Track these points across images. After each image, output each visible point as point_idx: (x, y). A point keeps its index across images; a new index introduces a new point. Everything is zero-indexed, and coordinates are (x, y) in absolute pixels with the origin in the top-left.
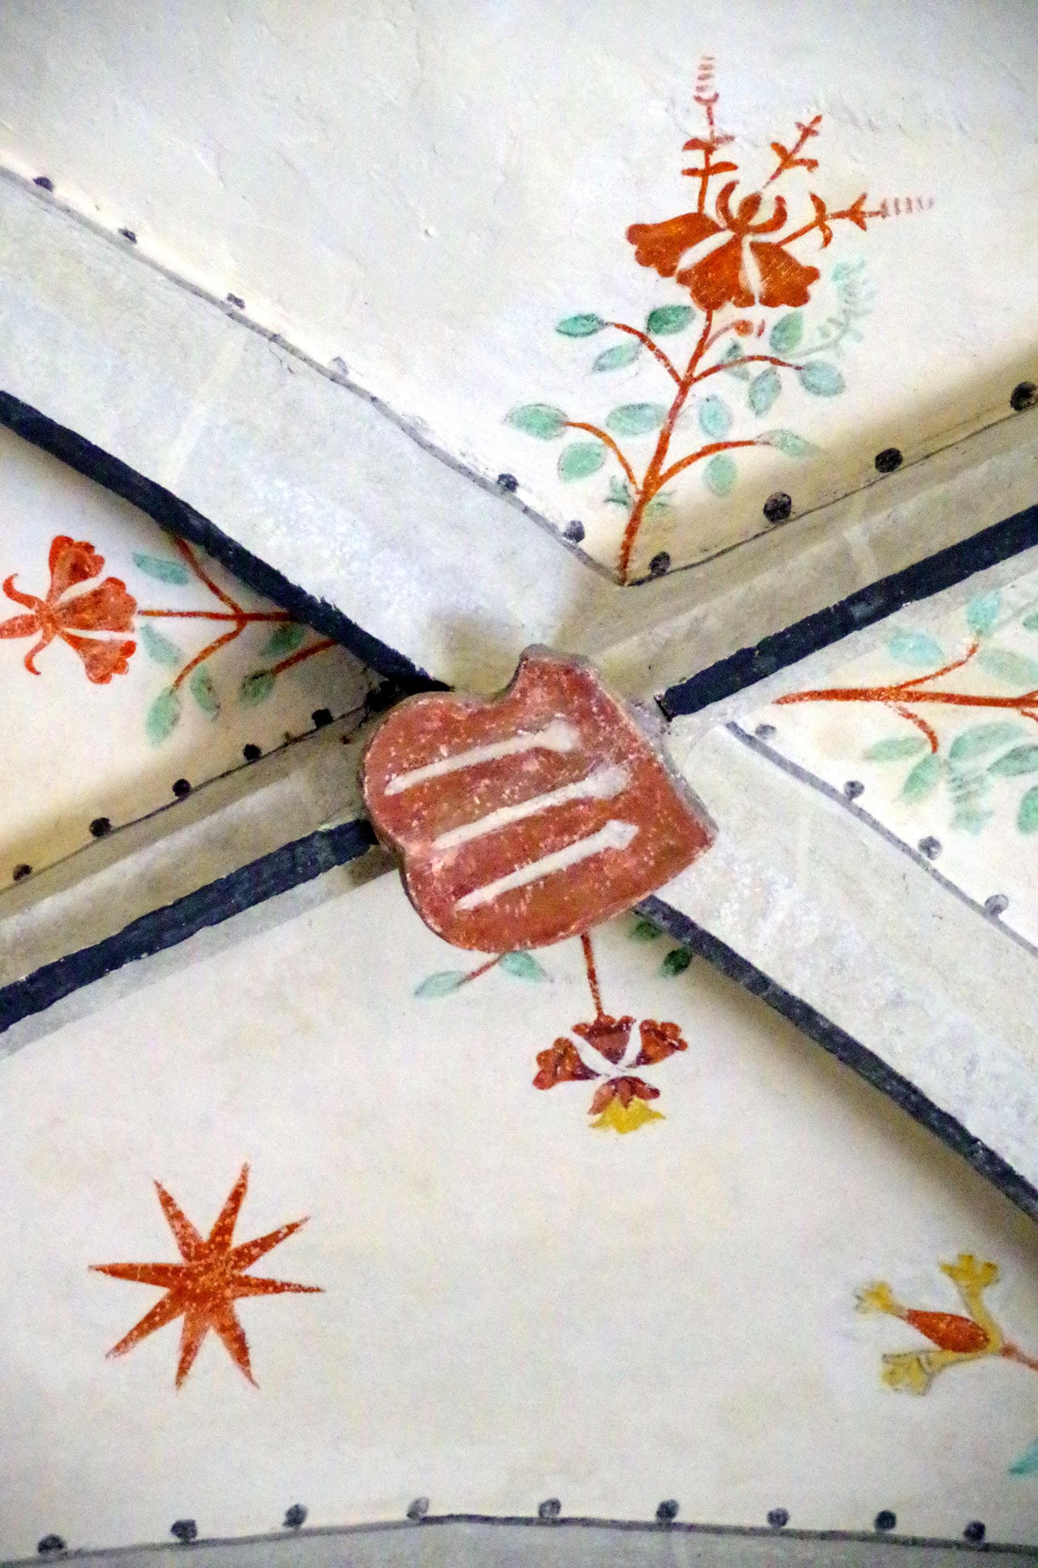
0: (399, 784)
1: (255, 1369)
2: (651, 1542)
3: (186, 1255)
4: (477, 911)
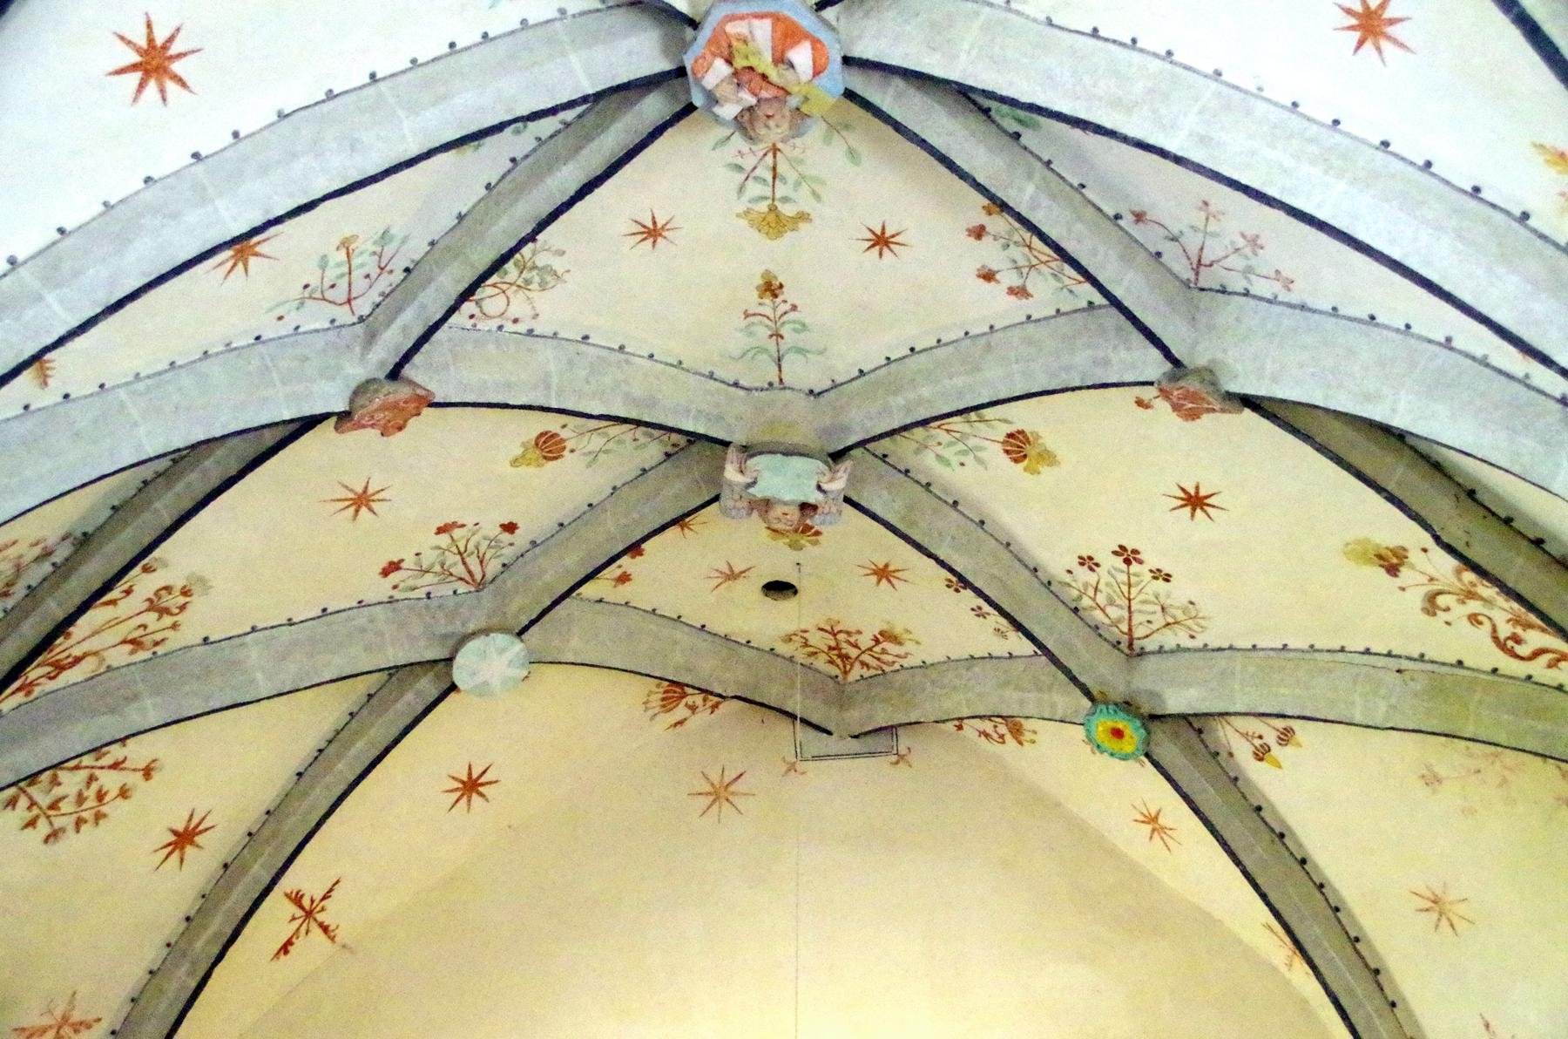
2: (372, 90)
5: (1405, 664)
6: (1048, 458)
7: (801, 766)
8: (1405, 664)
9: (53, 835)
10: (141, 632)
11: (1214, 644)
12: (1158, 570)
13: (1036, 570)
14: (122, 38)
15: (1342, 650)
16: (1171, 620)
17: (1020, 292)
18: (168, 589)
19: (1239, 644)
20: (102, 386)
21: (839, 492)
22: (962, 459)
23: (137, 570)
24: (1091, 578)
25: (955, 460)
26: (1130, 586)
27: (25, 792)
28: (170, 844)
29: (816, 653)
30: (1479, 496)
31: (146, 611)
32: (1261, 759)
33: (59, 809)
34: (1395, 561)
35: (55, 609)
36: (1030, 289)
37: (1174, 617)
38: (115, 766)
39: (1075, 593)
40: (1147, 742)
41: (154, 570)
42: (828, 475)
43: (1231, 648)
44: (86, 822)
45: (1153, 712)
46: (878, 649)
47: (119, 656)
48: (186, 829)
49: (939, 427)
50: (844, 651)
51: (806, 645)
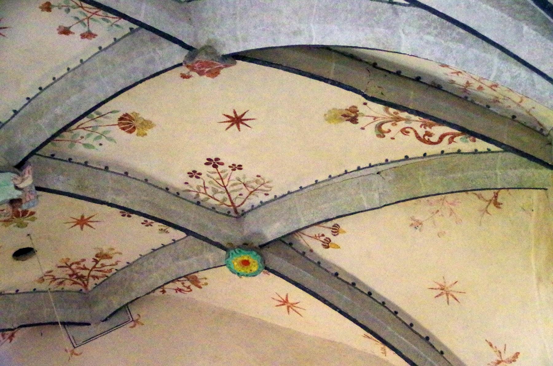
5: (380, 168)
6: (148, 124)
7: (77, 351)
8: (380, 168)
11: (279, 194)
12: (233, 165)
13: (167, 189)
15: (346, 172)
16: (252, 190)
17: (88, 35)
19: (292, 190)
21: (30, 186)
22: (101, 141)
24: (200, 182)
25: (96, 144)
26: (222, 179)
29: (63, 281)
30: (379, 65)
32: (328, 247)
34: (353, 115)
36: (93, 32)
37: (252, 187)
39: (194, 194)
40: (263, 261)
42: (19, 179)
43: (289, 193)
45: (261, 244)
46: (98, 265)
49: (78, 128)
50: (79, 274)
51: (54, 279)
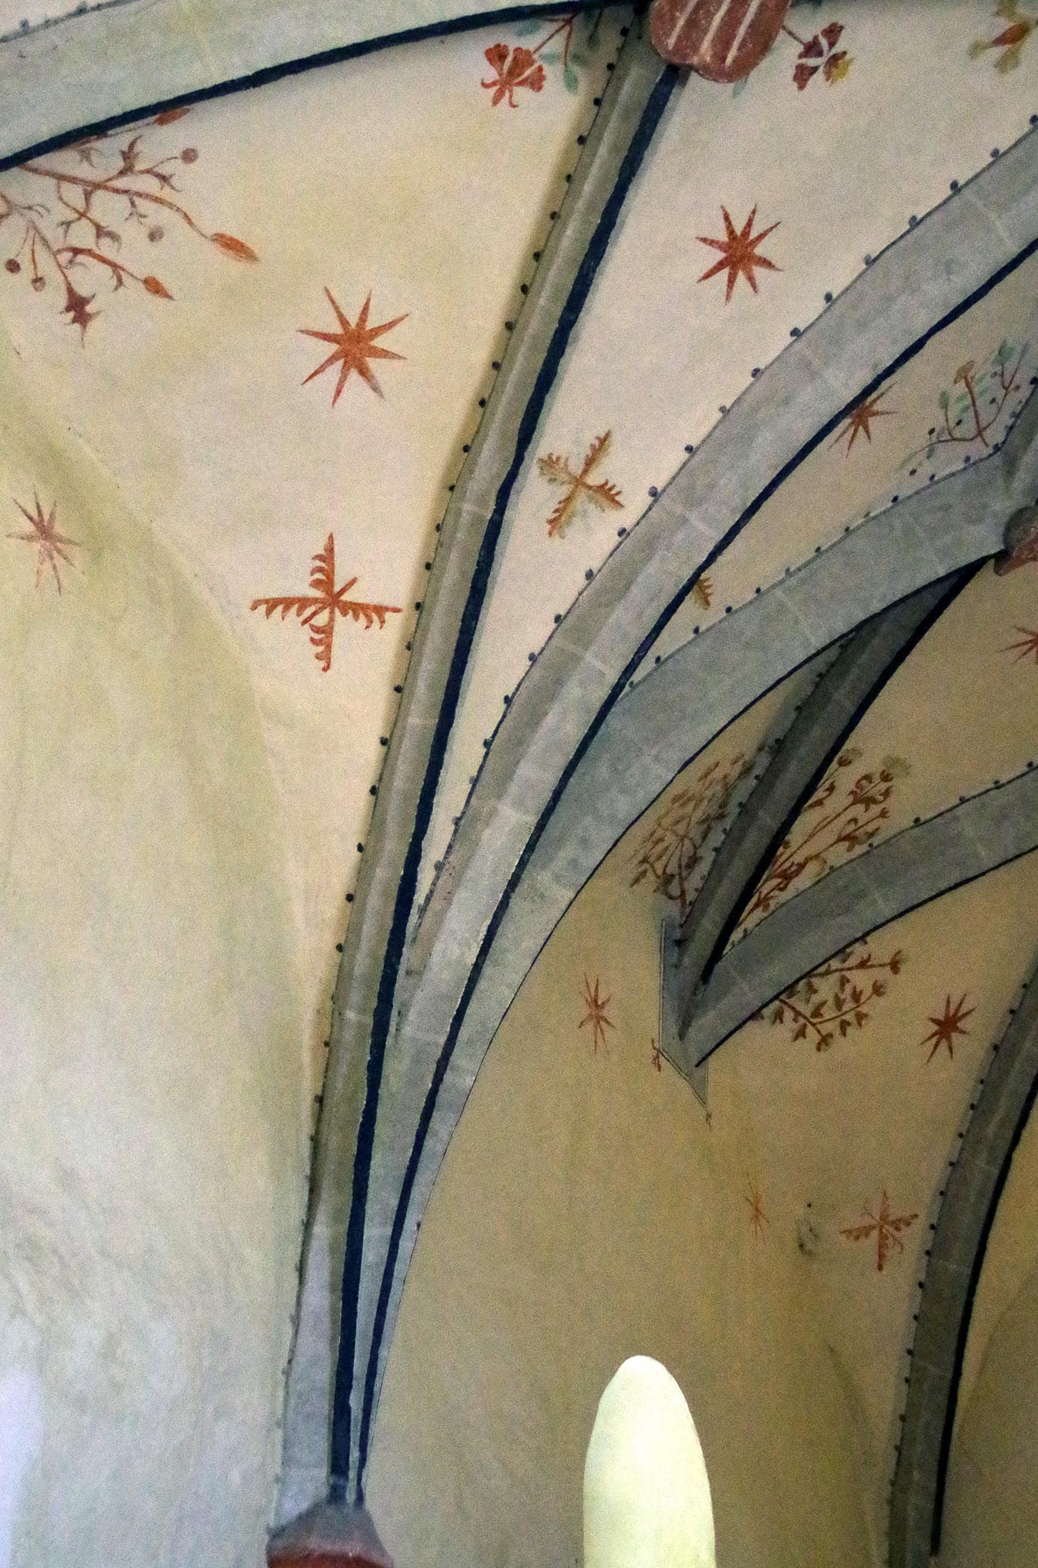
0: (672, 41)
1: (778, 265)
2: (956, 202)
3: (726, 251)
4: (734, 61)
9: (824, 1041)
10: (852, 827)
14: (704, 240)
18: (868, 778)
20: (758, 591)
23: (834, 764)
27: (786, 1003)
28: (934, 1035)
31: (852, 805)
33: (821, 1015)
35: (768, 819)
38: (863, 965)
41: (850, 762)
44: (849, 1024)
47: (839, 855)
48: (947, 1016)
